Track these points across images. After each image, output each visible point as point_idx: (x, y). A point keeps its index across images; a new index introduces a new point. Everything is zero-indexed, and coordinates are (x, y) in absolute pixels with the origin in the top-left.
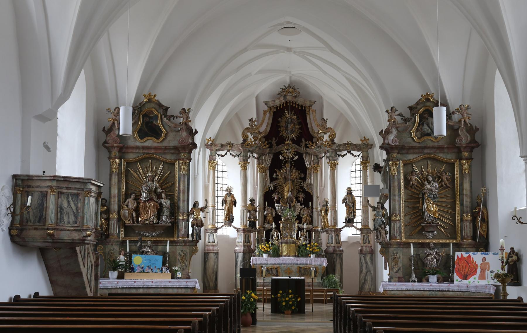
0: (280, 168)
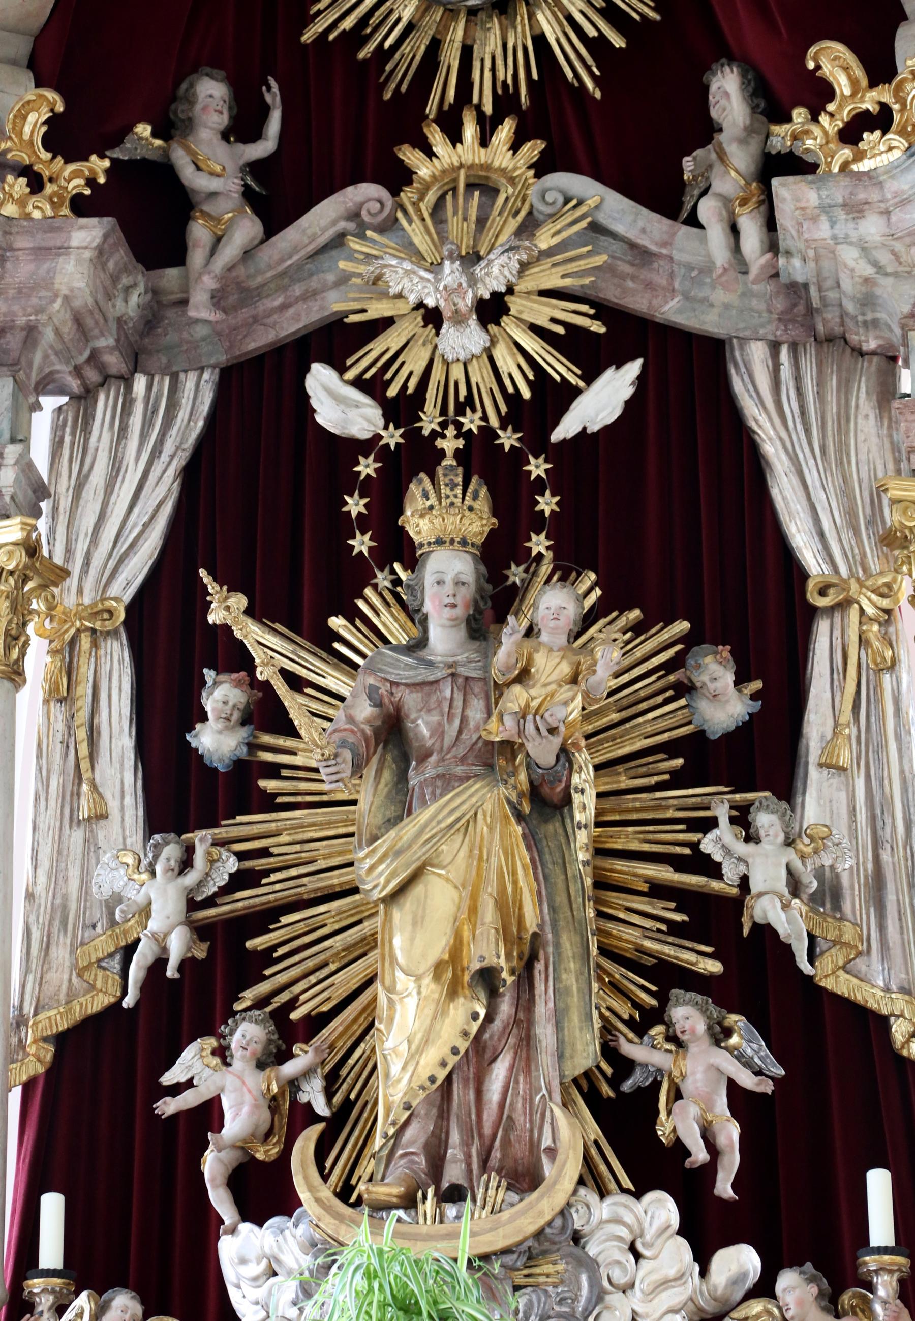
0: (314, 588)
